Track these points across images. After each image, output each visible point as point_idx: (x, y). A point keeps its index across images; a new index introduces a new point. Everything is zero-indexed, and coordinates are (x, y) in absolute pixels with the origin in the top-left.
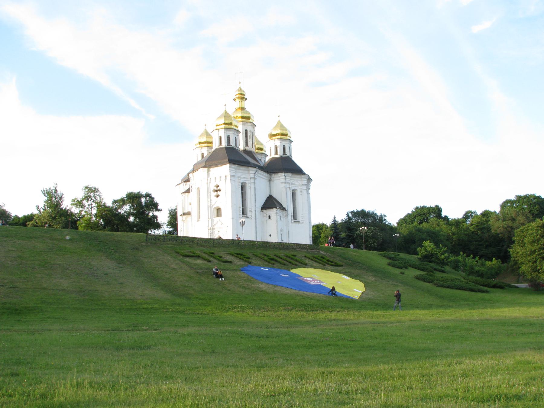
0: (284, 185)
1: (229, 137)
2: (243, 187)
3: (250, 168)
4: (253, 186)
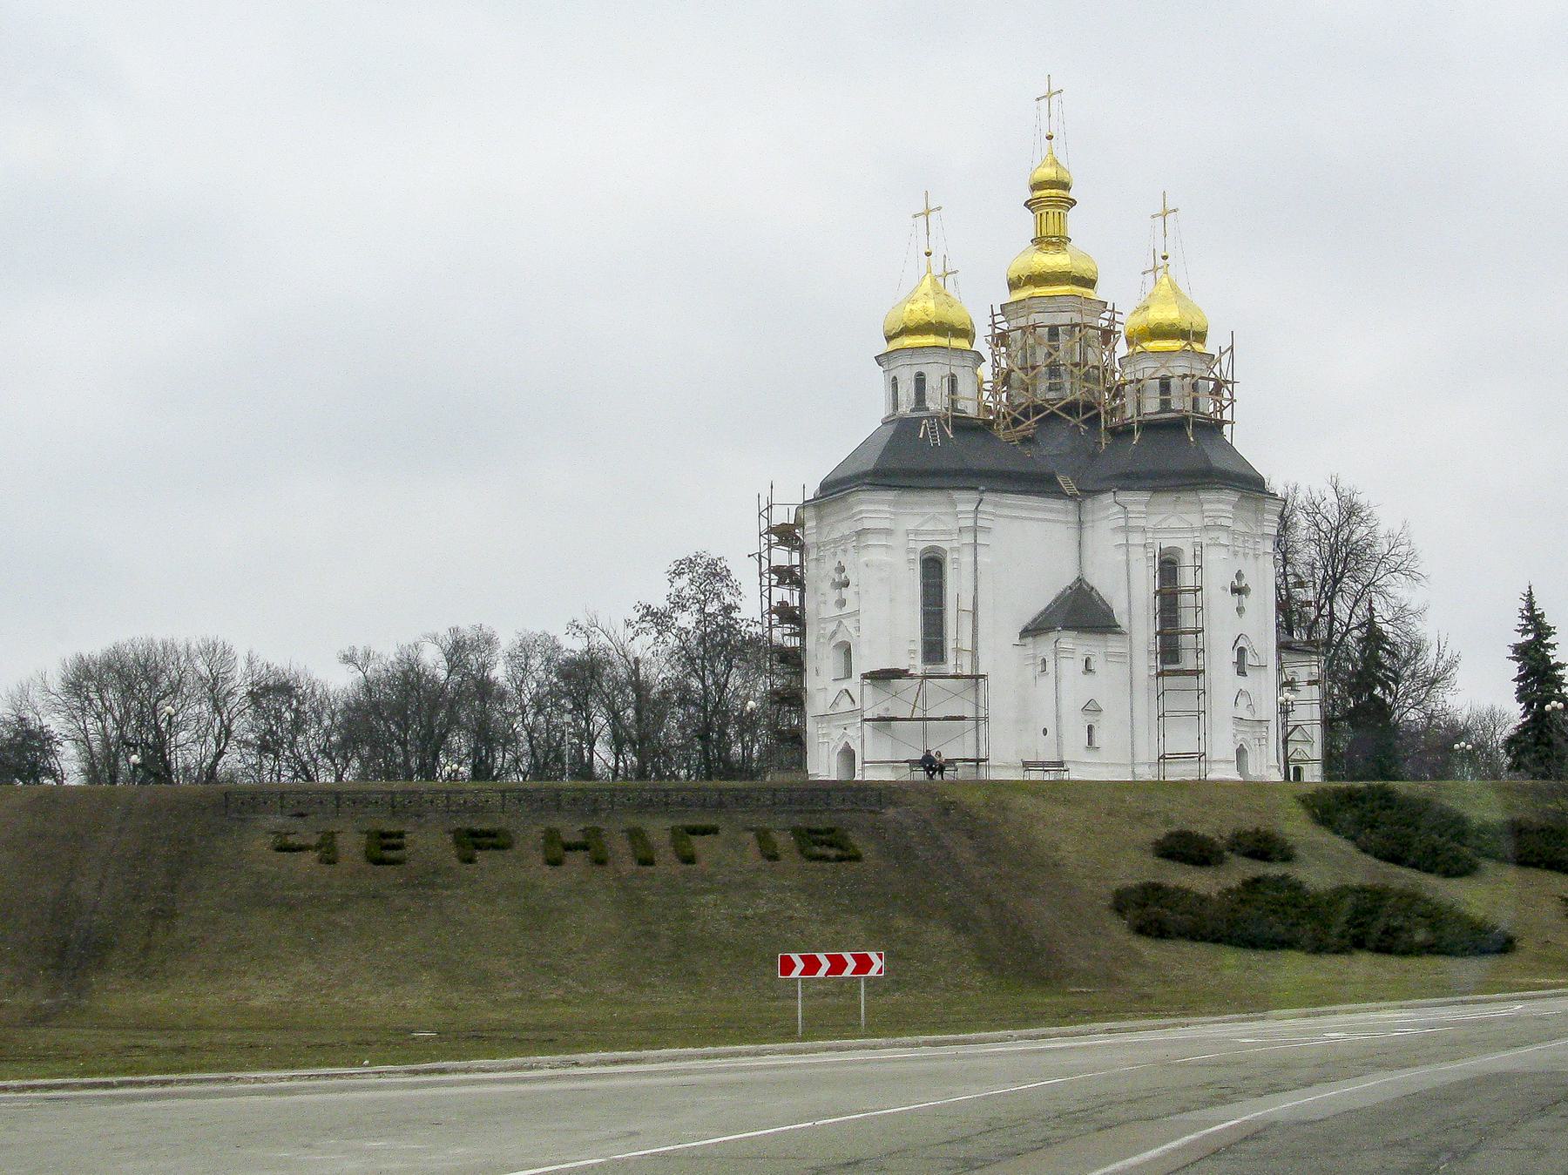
0: (1120, 539)
1: (920, 380)
2: (933, 567)
3: (957, 495)
4: (967, 558)
